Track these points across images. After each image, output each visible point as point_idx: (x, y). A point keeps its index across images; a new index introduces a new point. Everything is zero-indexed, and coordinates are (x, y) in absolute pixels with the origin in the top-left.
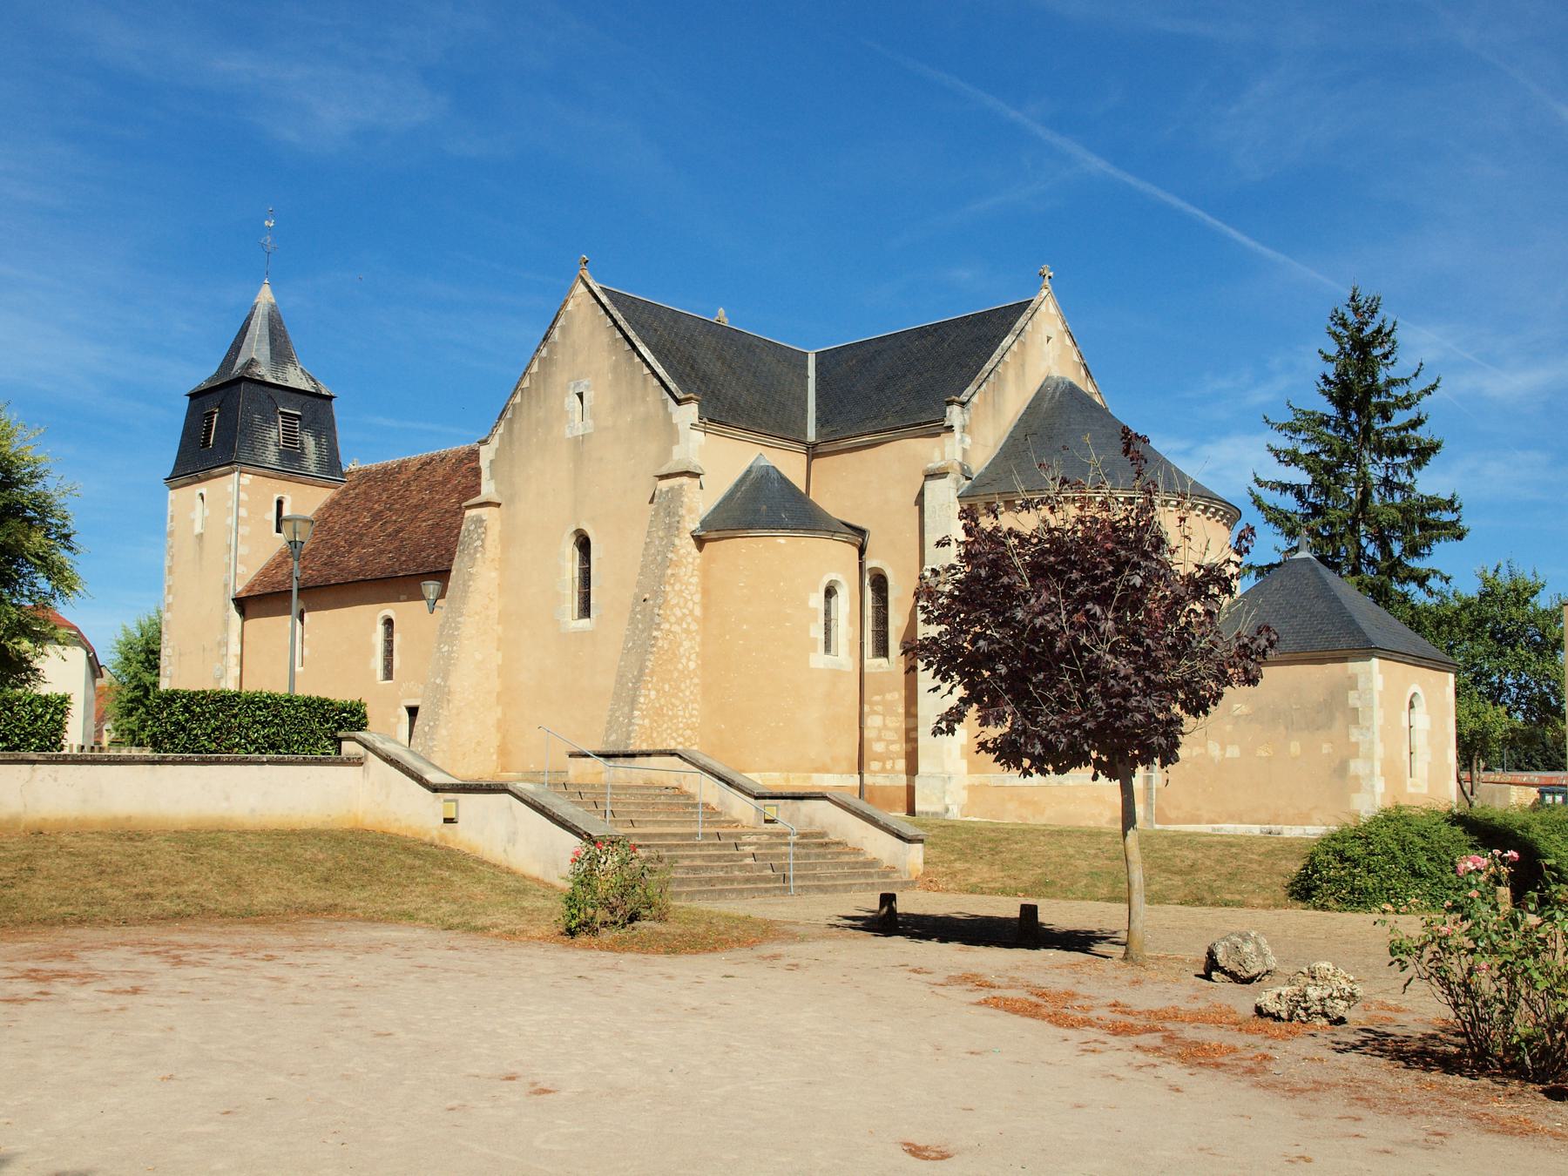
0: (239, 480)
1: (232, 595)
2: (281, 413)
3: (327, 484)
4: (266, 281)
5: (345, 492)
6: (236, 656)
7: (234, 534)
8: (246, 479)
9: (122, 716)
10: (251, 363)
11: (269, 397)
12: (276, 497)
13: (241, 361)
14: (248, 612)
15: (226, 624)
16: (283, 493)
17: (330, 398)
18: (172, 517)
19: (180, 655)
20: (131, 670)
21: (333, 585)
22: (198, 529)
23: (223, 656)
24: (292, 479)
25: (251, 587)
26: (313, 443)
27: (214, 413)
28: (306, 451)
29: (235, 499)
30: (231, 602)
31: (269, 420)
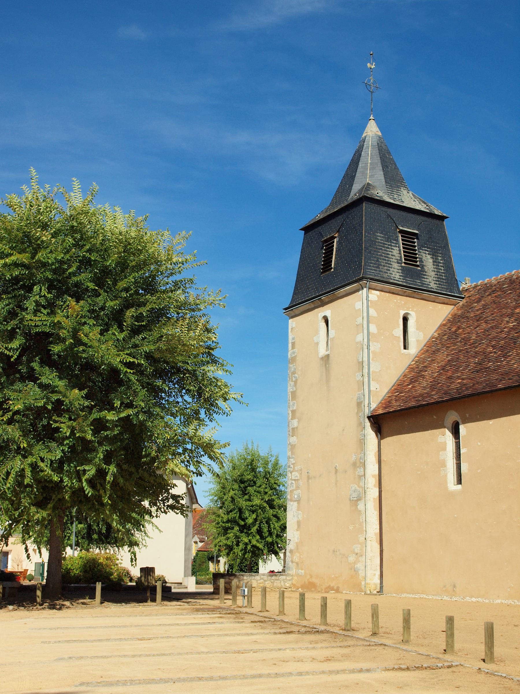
0: (367, 296)
1: (367, 412)
2: (401, 232)
3: (446, 300)
4: (372, 117)
5: (468, 307)
6: (373, 476)
7: (366, 351)
8: (374, 295)
9: (218, 534)
11: (389, 216)
12: (402, 313)
13: (356, 187)
14: (385, 429)
15: (362, 443)
16: (408, 309)
17: (442, 218)
18: (293, 344)
19: (309, 478)
20: (227, 497)
21: (501, 389)
22: (322, 351)
23: (360, 477)
25: (387, 403)
26: (431, 261)
27: (333, 238)
28: (426, 269)
29: (365, 315)
30: (367, 420)
31: (390, 239)
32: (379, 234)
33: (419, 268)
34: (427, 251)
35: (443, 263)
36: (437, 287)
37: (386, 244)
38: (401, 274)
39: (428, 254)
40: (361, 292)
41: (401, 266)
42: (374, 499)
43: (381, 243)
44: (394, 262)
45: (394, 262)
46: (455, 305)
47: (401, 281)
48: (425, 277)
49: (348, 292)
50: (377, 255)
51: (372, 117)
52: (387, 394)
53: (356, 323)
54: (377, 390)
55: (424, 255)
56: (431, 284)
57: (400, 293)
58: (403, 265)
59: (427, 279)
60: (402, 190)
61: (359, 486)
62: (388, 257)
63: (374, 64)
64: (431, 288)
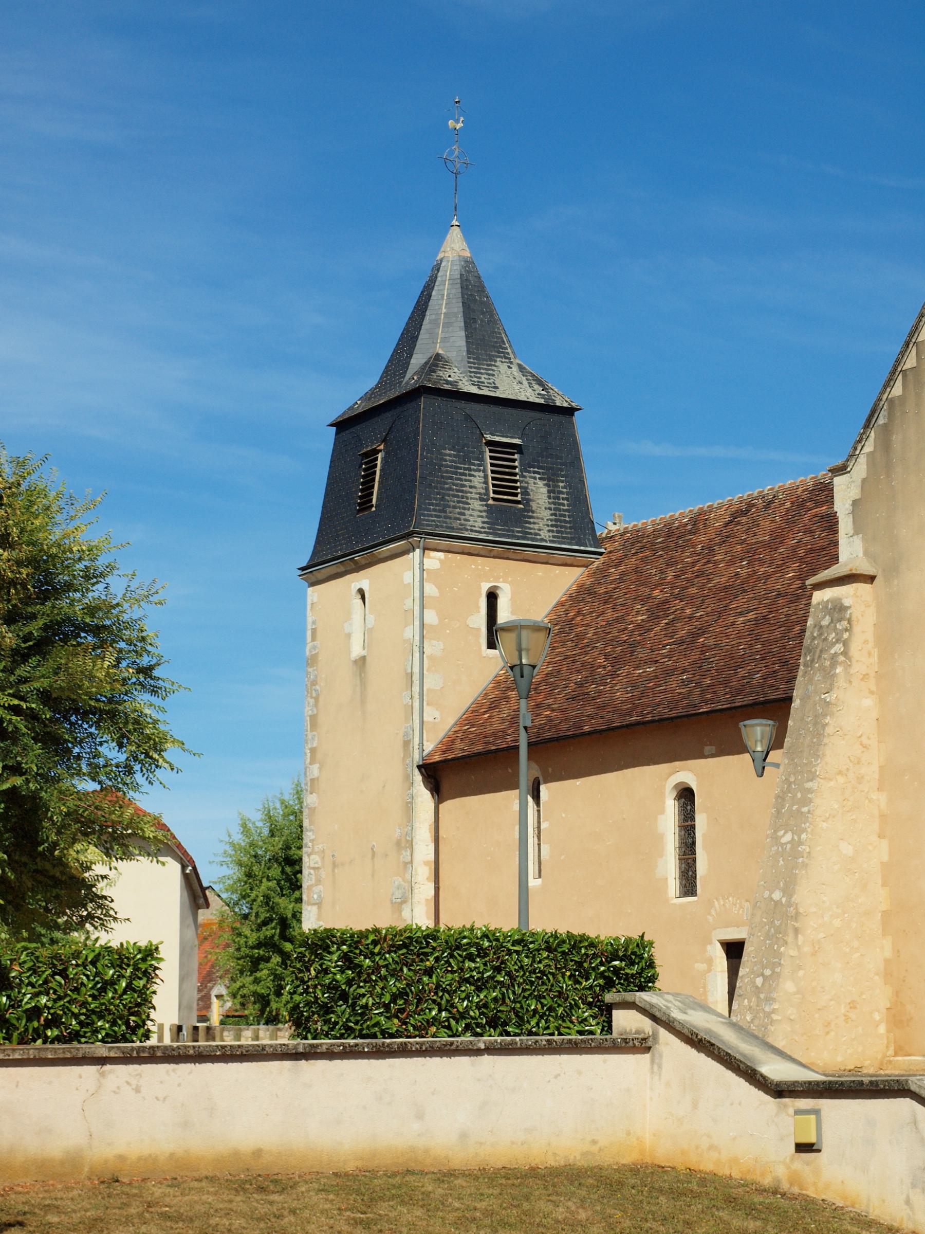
0: (422, 563)
1: (417, 759)
2: (489, 443)
3: (569, 560)
4: (455, 222)
5: (602, 572)
6: (426, 863)
7: (417, 655)
8: (434, 560)
9: (242, 972)
10: (437, 361)
11: (468, 417)
12: (485, 587)
13: (418, 360)
14: (445, 787)
15: (409, 807)
16: (497, 579)
17: (570, 411)
18: (314, 632)
19: (334, 865)
20: (258, 894)
21: (589, 733)
22: (357, 650)
23: (406, 864)
24: (510, 555)
25: (448, 744)
26: (544, 490)
27: (376, 452)
28: (534, 505)
29: (417, 594)
30: (417, 772)
31: (469, 457)
32: (448, 452)
33: (521, 506)
34: (538, 473)
35: (567, 493)
36: (553, 536)
37: (460, 468)
38: (486, 520)
39: (540, 479)
40: (411, 554)
41: (487, 505)
42: (427, 900)
43: (451, 467)
44: (474, 499)
45: (474, 499)
46: (587, 567)
47: (485, 532)
48: (532, 520)
49: (393, 552)
50: (443, 489)
51: (455, 222)
52: (453, 727)
53: (405, 607)
54: (436, 720)
55: (531, 481)
56: (541, 533)
57: (482, 553)
58: (491, 502)
59: (534, 523)
60: (497, 364)
61: (404, 880)
62: (462, 491)
63: (462, 119)
64: (542, 540)
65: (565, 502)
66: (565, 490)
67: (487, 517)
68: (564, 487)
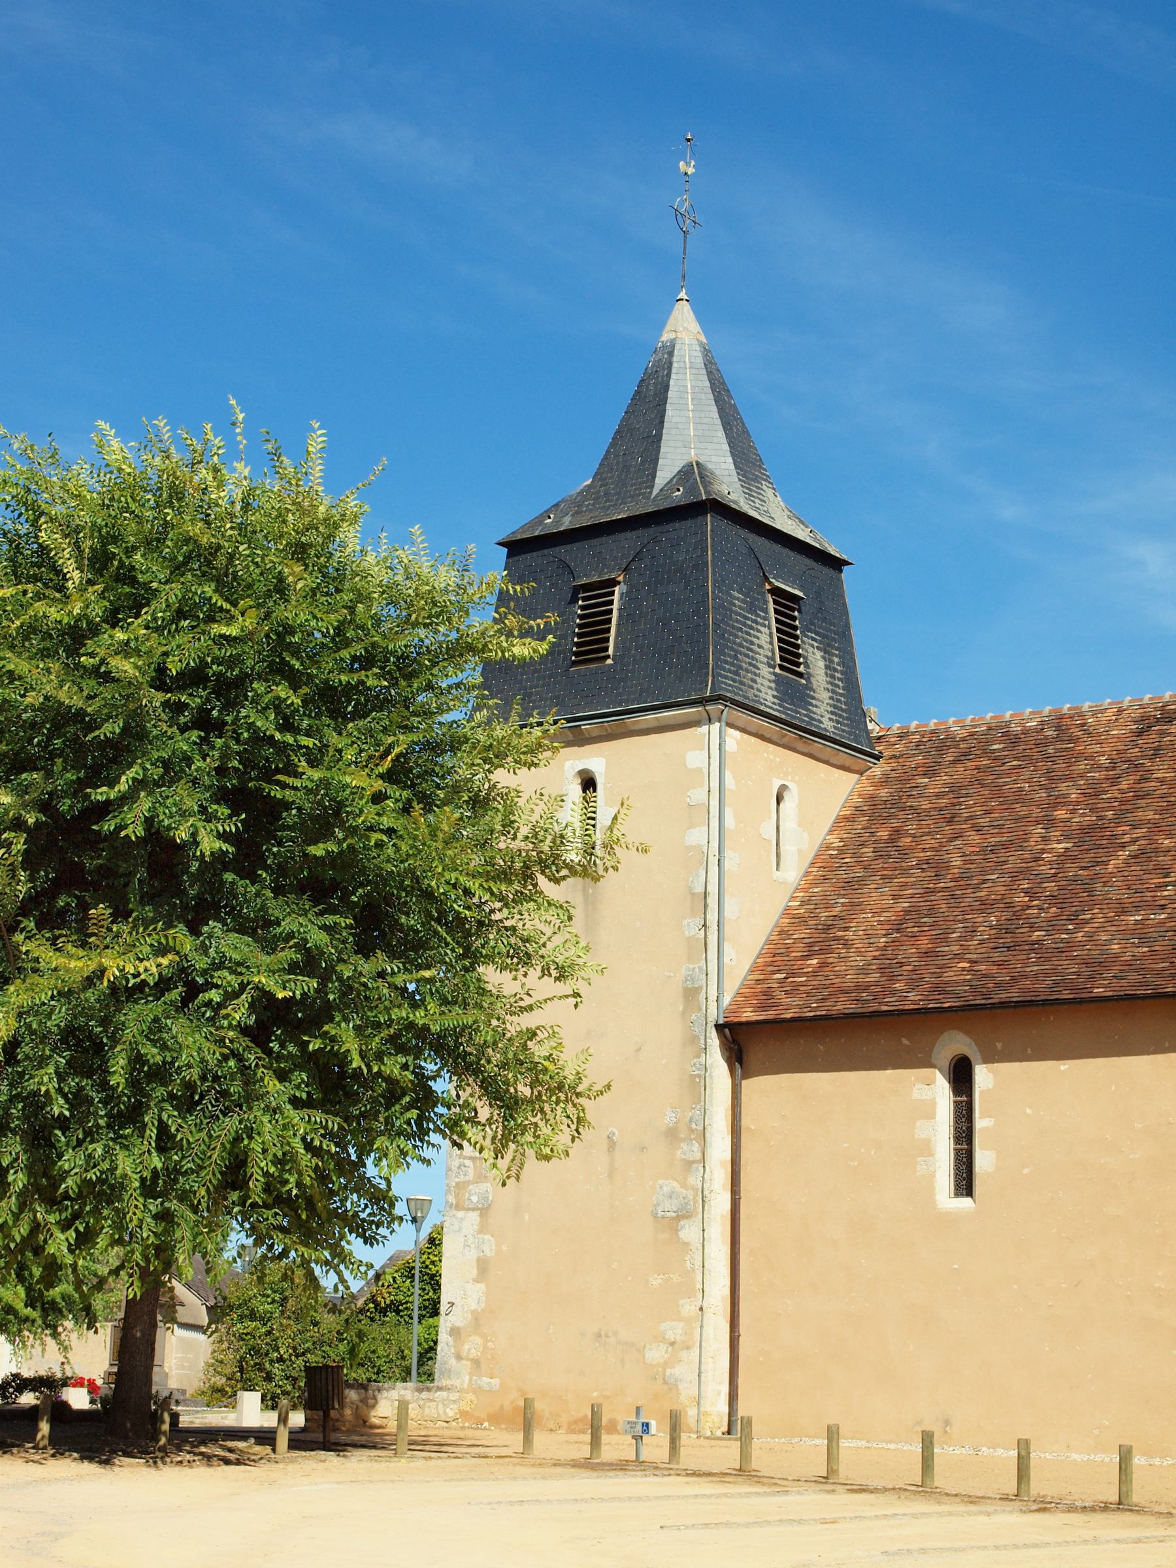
2: (776, 591)
5: (901, 780)
10: (691, 473)
15: (698, 1085)
17: (837, 564)
23: (689, 1164)
24: (800, 746)
26: (821, 664)
27: (614, 583)
30: (713, 1033)
32: (735, 594)
33: (803, 681)
34: (815, 640)
35: (842, 673)
36: (835, 728)
37: (748, 619)
38: (775, 693)
39: (818, 648)
40: (705, 728)
41: (775, 674)
42: (722, 1216)
43: (740, 614)
44: (762, 663)
45: (762, 663)
46: (862, 774)
47: (777, 710)
48: (814, 702)
49: (663, 724)
50: (735, 643)
51: (683, 295)
52: (748, 974)
53: (688, 800)
54: (732, 963)
55: (810, 649)
56: (823, 720)
57: (775, 738)
58: (777, 670)
59: (816, 706)
60: (764, 488)
61: (684, 1185)
62: (751, 650)
63: (693, 163)
64: (825, 729)
65: (840, 683)
66: (839, 668)
67: (776, 690)
68: (838, 664)
